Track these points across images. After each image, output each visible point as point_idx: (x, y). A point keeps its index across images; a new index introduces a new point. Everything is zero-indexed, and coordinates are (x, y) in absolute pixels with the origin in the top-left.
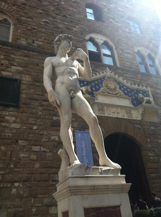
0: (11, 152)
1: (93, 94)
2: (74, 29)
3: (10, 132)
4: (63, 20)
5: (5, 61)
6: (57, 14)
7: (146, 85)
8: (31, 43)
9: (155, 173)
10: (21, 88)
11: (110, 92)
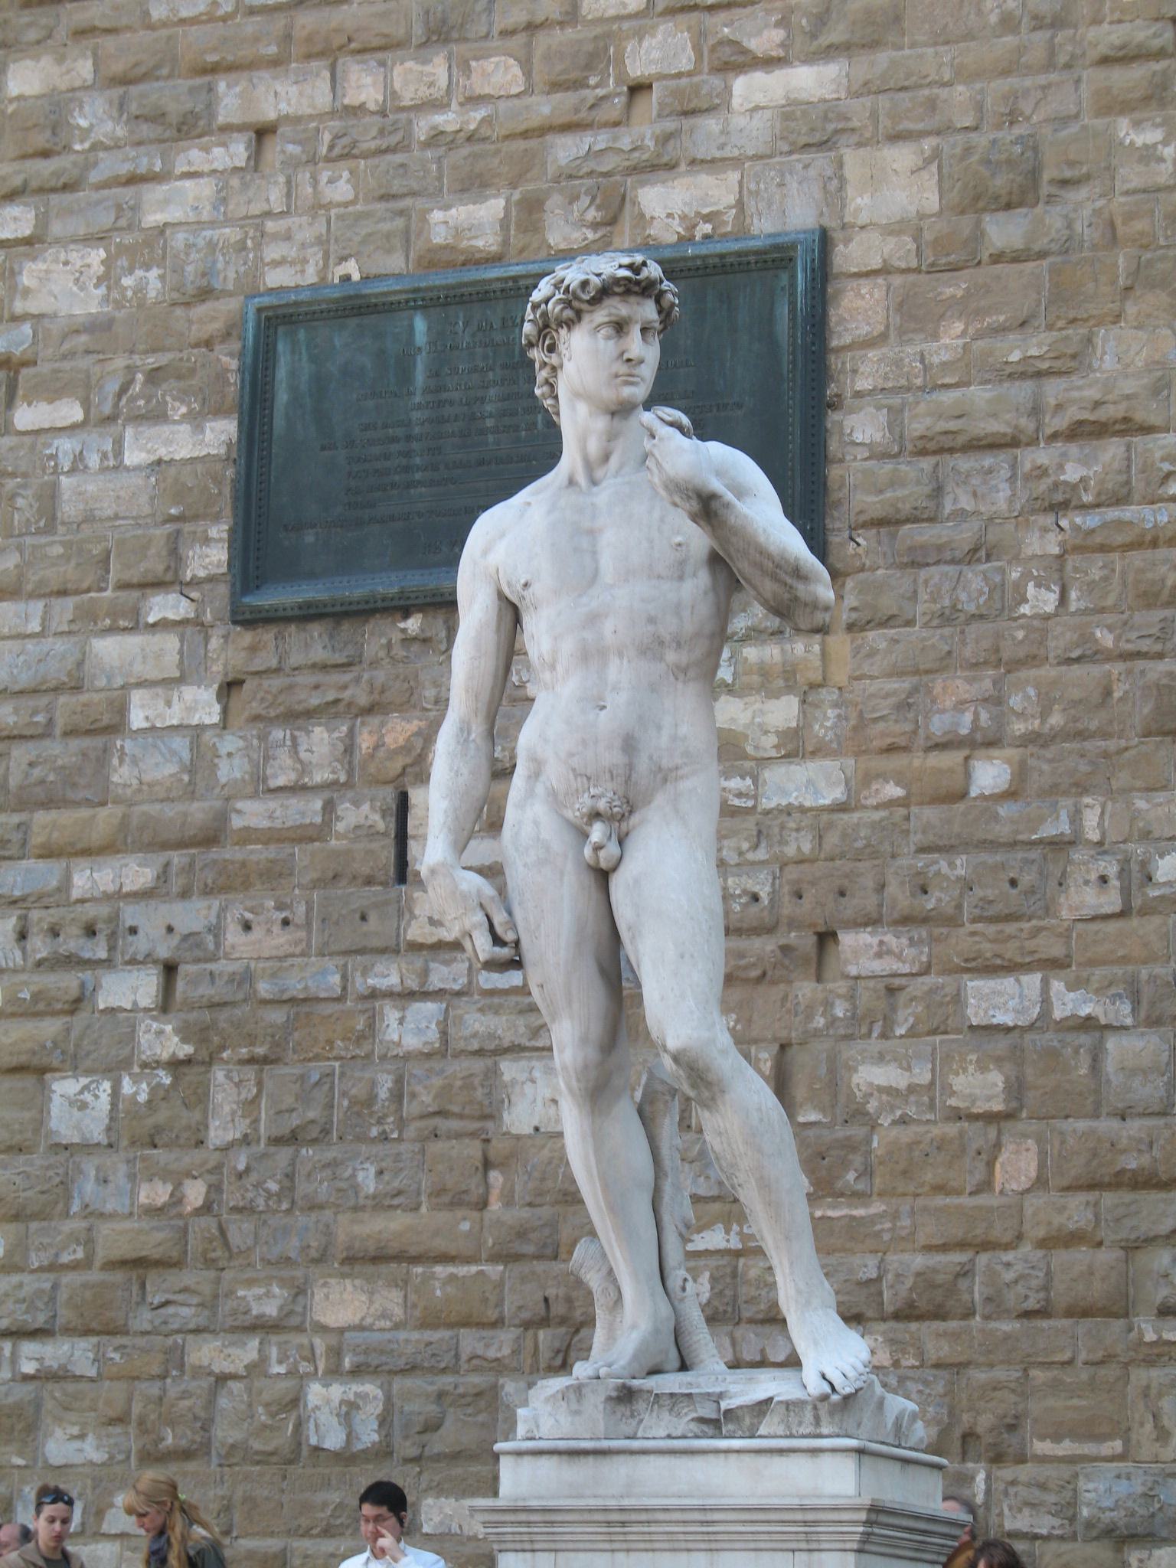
0: (783, 1047)
3: (761, 854)
5: (665, 27)
10: (834, 343)
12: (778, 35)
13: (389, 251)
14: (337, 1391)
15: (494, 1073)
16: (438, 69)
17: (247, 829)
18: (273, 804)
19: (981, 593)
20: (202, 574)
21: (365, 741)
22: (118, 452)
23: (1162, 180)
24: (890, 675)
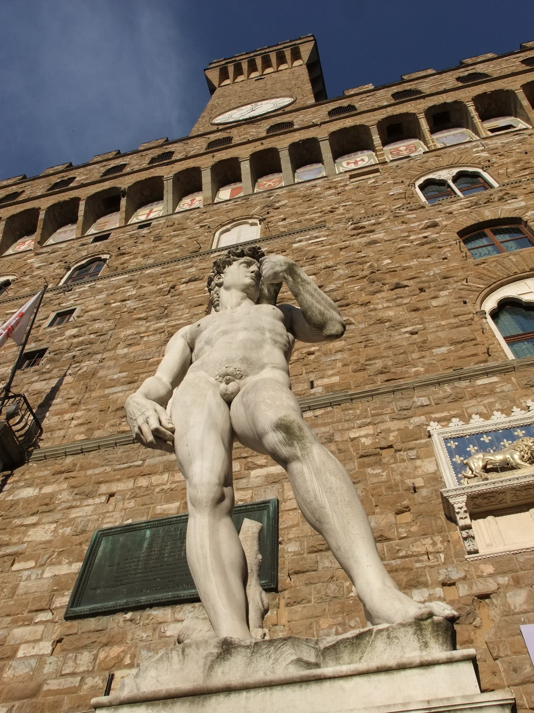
2: (434, 303)
4: (395, 296)
6: (375, 293)
8: (303, 392)
10: (281, 527)
12: (265, 461)
13: (142, 516)
16: (166, 476)
17: (49, 690)
18: (62, 680)
19: (335, 590)
20: (58, 605)
21: (102, 655)
22: (42, 574)
23: (383, 480)
24: (302, 619)
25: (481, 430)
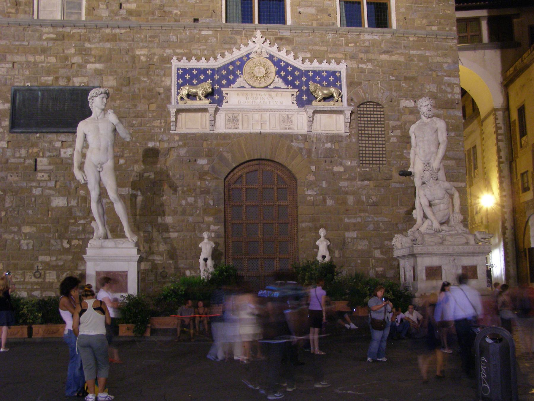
1: (222, 92)
7: (339, 56)
9: (309, 222)
11: (255, 85)
14: (26, 241)
15: (49, 198)
16: (43, 57)
18: (16, 159)
21: (30, 151)
25: (194, 67)
